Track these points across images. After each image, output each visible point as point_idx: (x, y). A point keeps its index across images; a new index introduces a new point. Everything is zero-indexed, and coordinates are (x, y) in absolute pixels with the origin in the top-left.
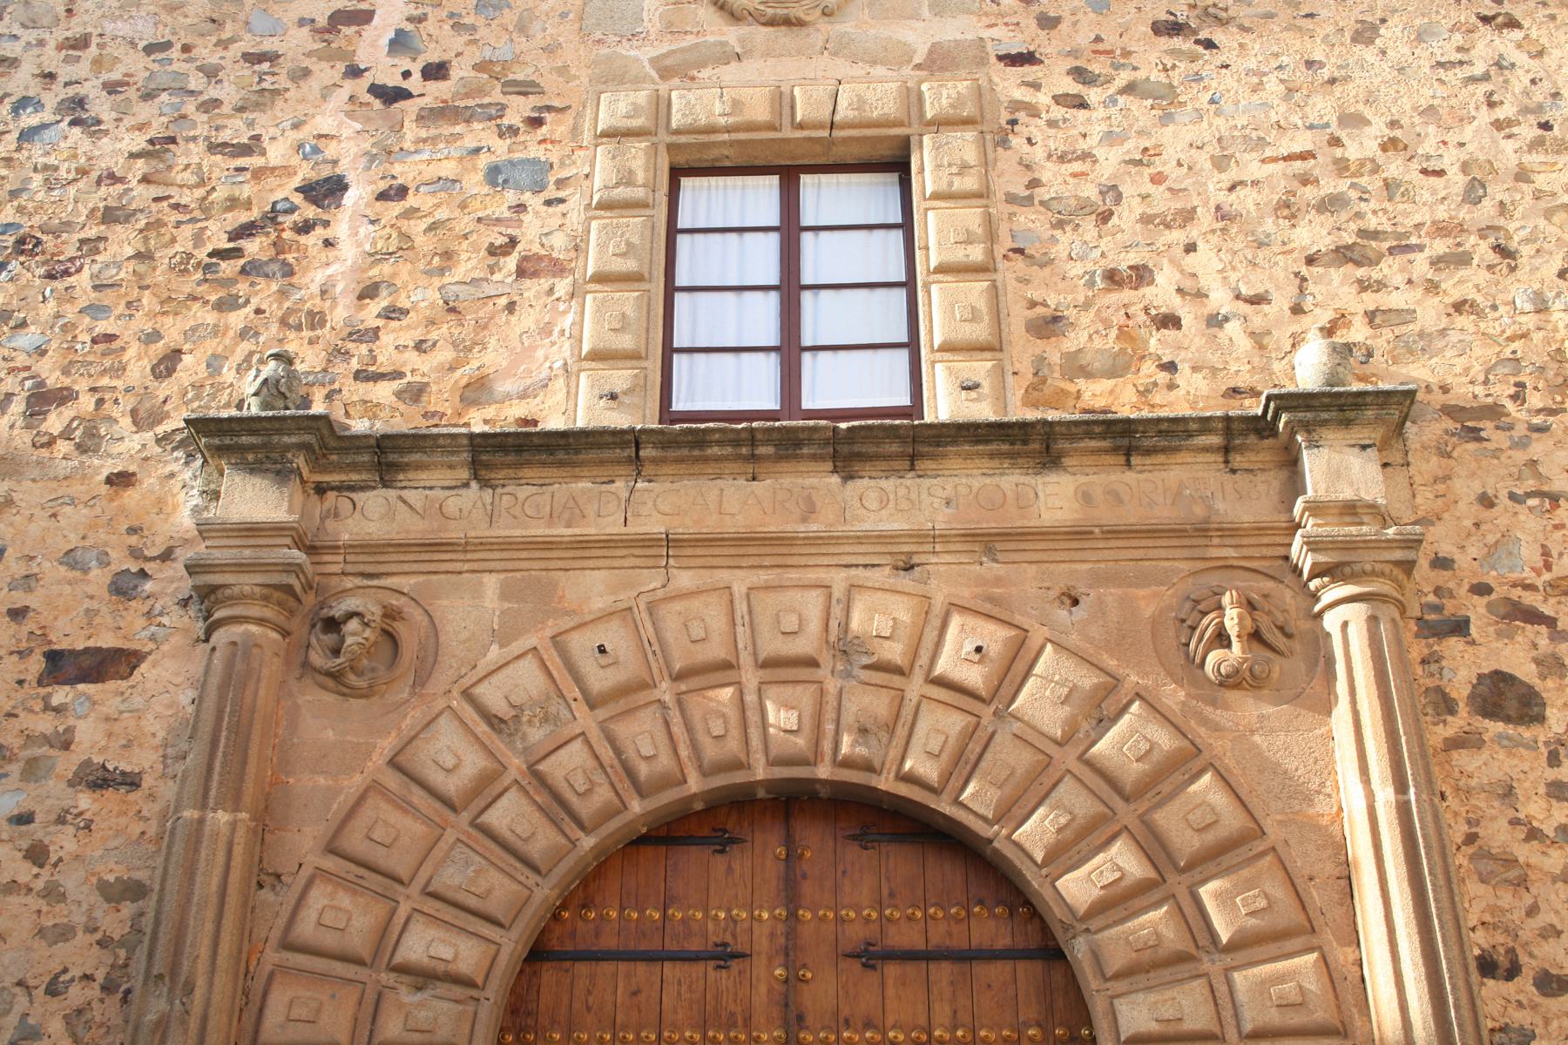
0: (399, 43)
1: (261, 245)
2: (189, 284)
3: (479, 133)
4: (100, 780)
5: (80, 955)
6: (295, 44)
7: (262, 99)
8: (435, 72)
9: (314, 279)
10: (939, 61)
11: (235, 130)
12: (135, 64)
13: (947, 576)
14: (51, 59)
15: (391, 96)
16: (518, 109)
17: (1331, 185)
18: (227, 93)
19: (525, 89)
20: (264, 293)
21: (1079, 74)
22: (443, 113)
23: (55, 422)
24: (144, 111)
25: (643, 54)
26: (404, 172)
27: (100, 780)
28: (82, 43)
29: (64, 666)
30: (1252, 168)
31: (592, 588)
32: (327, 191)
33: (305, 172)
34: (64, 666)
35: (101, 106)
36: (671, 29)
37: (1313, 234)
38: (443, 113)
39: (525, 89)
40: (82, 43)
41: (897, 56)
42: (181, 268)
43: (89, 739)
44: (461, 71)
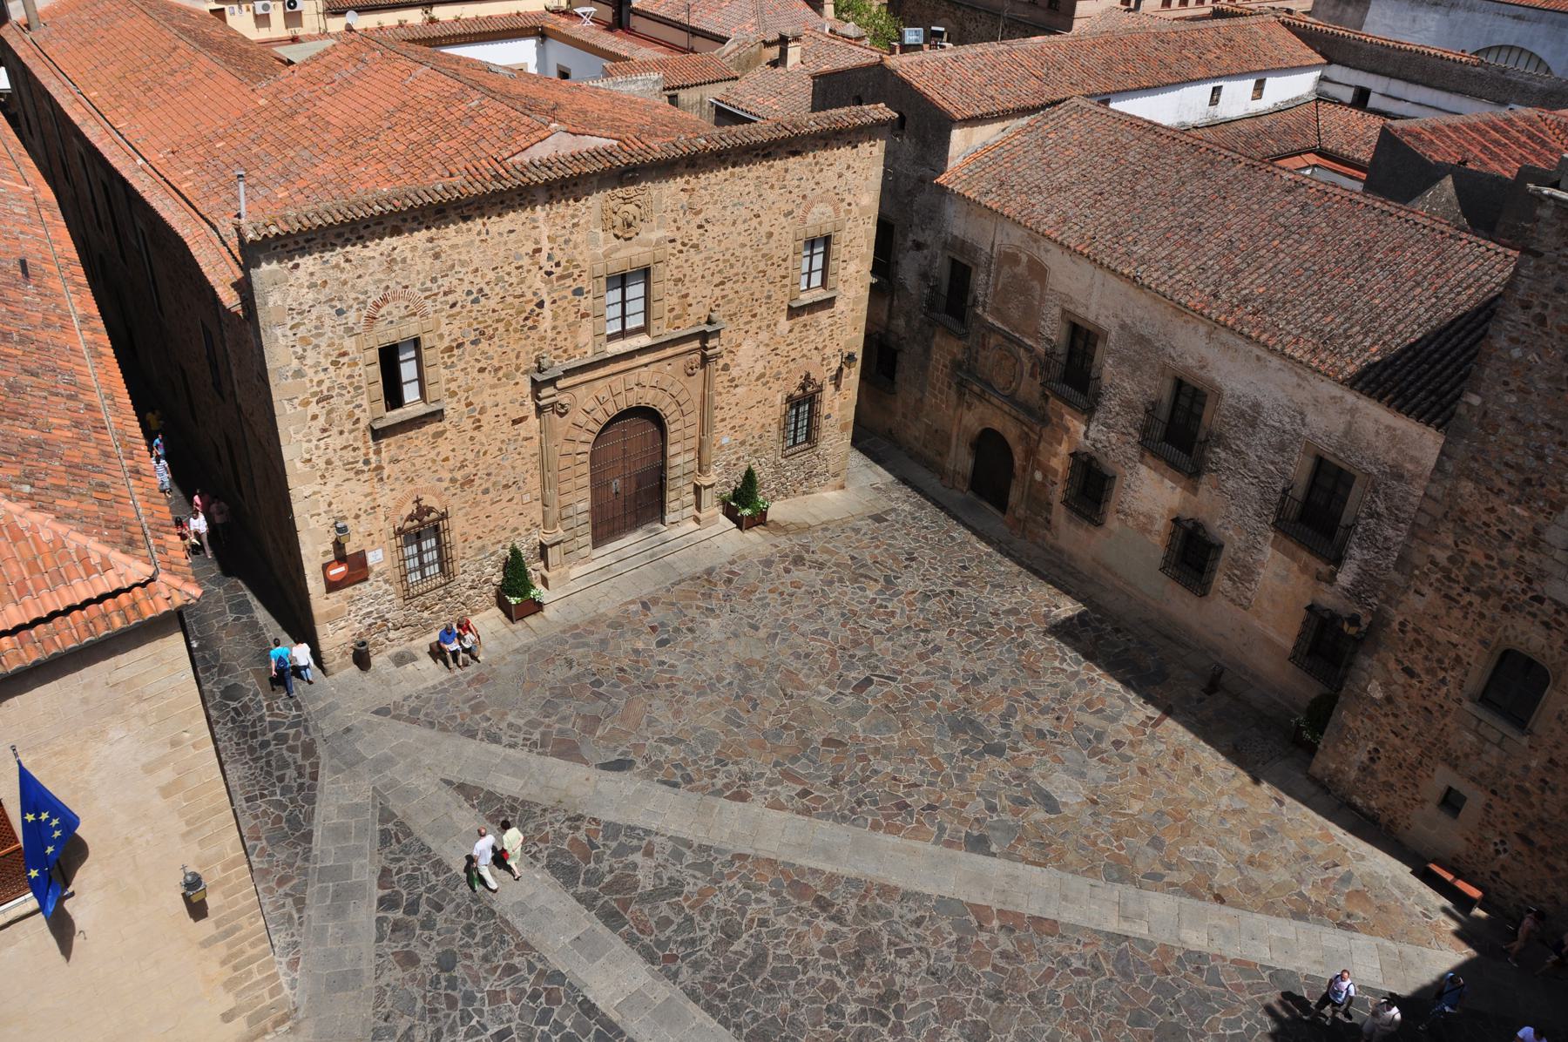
0: (550, 257)
1: (530, 319)
2: (518, 335)
3: (569, 282)
4: (526, 439)
5: (529, 466)
6: (526, 261)
7: (522, 282)
8: (558, 265)
9: (541, 328)
10: (658, 243)
11: (518, 292)
12: (491, 275)
13: (652, 368)
14: (471, 277)
15: (549, 274)
16: (577, 272)
17: (721, 266)
18: (514, 280)
19: (577, 266)
20: (533, 334)
21: (684, 244)
22: (561, 278)
23: (500, 374)
24: (497, 289)
25: (600, 251)
26: (555, 295)
27: (526, 439)
28: (476, 270)
29: (515, 422)
30: (709, 264)
31: (600, 384)
32: (541, 305)
33: (536, 300)
34: (515, 422)
35: (487, 290)
36: (606, 241)
37: (717, 280)
38: (561, 278)
39: (577, 266)
40: (476, 270)
41: (647, 244)
42: (516, 331)
43: (523, 434)
44: (563, 264)
